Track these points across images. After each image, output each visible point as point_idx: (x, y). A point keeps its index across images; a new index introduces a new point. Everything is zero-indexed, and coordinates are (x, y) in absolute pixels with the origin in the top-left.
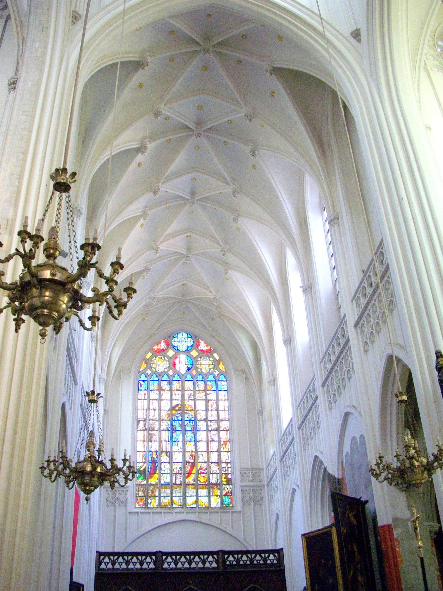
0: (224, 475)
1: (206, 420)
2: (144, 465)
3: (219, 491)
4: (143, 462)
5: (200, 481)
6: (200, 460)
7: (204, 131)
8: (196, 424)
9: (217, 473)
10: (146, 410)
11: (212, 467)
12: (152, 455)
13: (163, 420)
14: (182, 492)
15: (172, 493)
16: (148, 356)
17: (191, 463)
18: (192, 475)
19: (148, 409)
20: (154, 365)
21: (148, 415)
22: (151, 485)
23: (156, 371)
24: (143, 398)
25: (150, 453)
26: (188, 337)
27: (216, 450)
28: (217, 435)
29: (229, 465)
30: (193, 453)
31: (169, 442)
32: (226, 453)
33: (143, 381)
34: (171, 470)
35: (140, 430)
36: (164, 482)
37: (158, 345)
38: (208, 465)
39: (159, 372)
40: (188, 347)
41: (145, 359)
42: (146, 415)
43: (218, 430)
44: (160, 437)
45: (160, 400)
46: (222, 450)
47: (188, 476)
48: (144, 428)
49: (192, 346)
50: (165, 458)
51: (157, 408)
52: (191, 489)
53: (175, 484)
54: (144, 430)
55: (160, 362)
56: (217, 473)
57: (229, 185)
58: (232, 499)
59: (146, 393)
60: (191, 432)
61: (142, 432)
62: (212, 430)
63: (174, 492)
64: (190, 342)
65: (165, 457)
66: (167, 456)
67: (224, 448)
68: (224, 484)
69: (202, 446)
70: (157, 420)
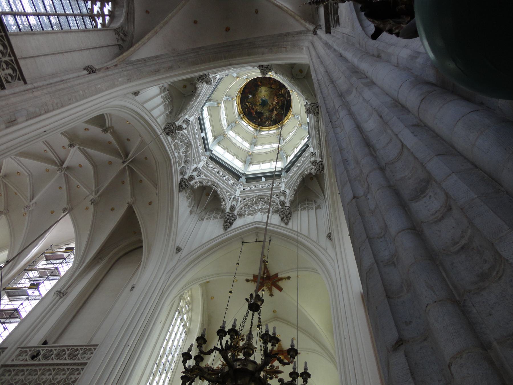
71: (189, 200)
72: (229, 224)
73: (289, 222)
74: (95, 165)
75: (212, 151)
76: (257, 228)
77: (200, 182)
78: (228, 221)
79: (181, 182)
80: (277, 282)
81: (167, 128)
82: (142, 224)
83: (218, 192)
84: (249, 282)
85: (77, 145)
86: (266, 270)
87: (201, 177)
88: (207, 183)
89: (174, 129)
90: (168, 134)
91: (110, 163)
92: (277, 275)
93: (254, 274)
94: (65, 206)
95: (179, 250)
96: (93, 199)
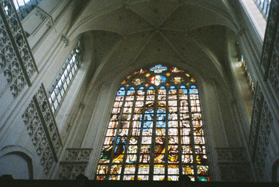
1: (177, 113)
2: (110, 147)
3: (193, 170)
5: (170, 161)
10: (121, 108)
11: (183, 148)
13: (135, 113)
14: (148, 170)
15: (137, 171)
17: (161, 144)
22: (115, 164)
24: (119, 100)
27: (188, 134)
28: (189, 123)
29: (204, 147)
31: (140, 129)
34: (139, 150)
36: (130, 161)
42: (120, 111)
43: (190, 120)
45: (134, 101)
46: (195, 134)
48: (117, 119)
52: (159, 168)
53: (142, 163)
54: (115, 121)
62: (183, 120)
63: (139, 170)
65: (134, 140)
66: (136, 139)
67: (197, 133)
69: (173, 132)
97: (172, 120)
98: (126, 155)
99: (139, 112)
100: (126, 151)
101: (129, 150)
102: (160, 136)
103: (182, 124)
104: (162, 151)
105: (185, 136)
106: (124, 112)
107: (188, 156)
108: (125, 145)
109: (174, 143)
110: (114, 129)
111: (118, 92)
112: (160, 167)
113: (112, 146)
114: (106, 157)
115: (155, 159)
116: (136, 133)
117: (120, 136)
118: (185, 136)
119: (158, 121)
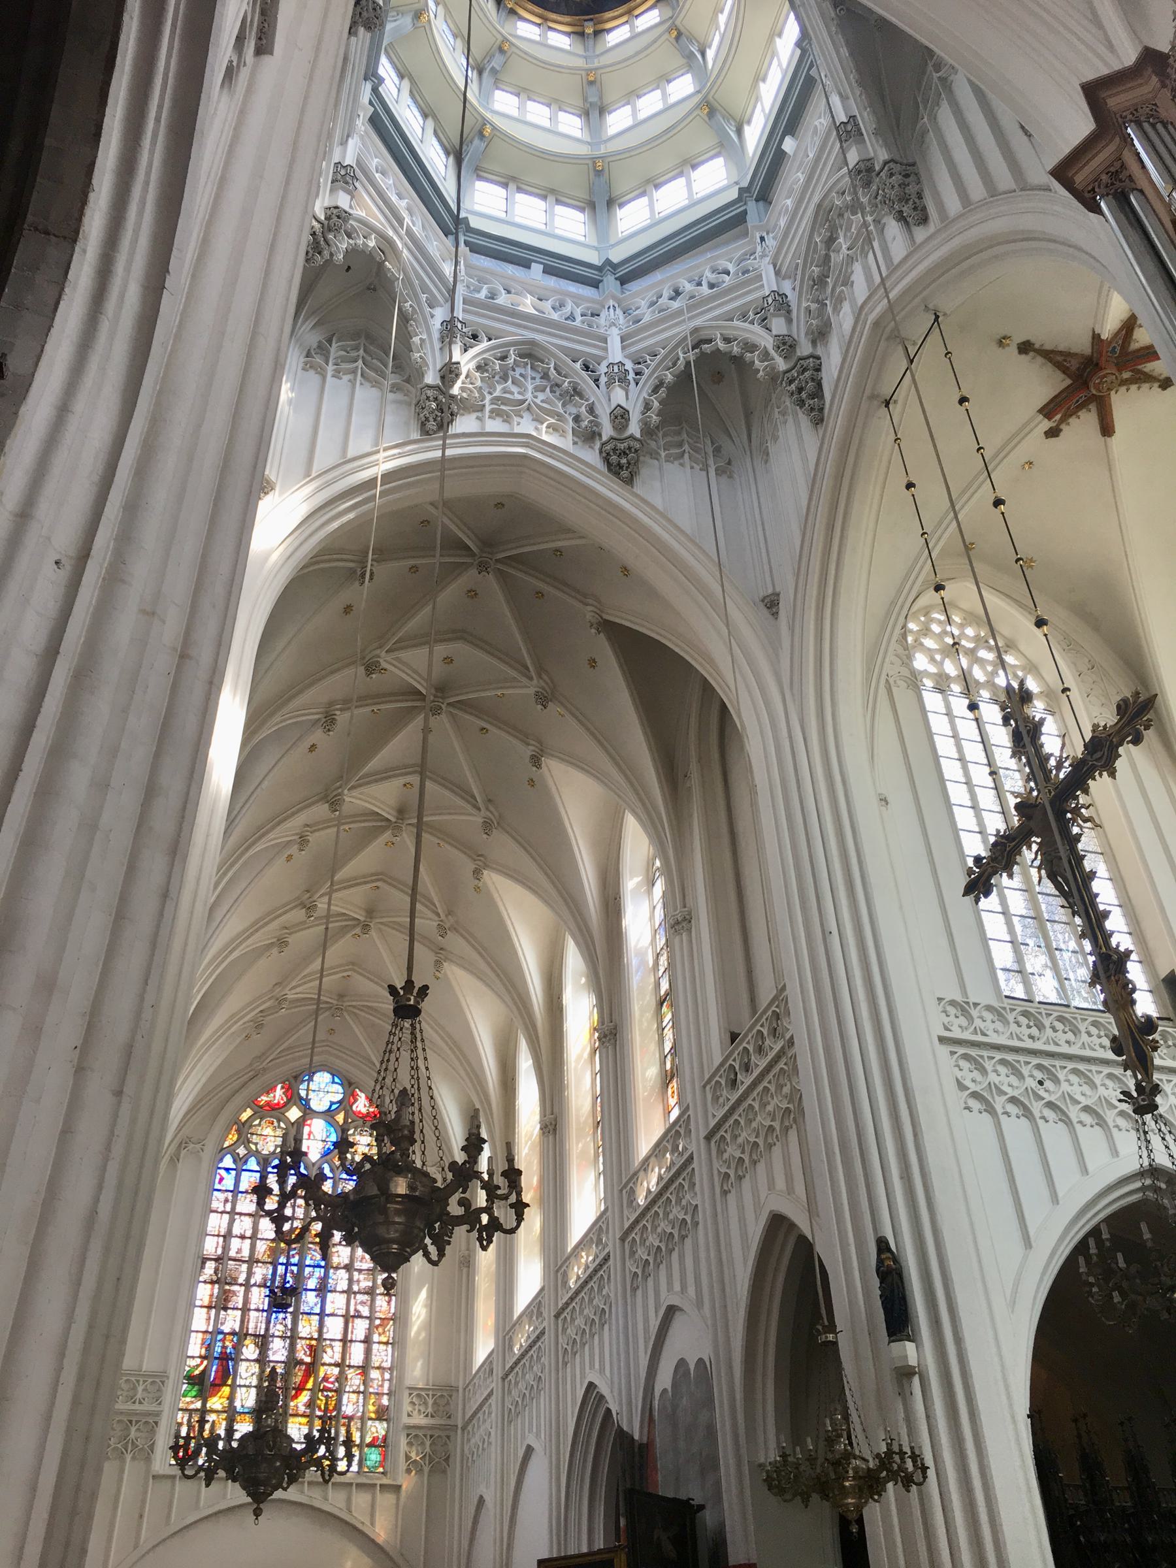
0: (373, 1396)
2: (202, 1363)
4: (200, 1357)
6: (326, 1359)
7: (448, 704)
8: (326, 1275)
9: (359, 1392)
10: (224, 1237)
11: (349, 1377)
12: (223, 1340)
13: (258, 1261)
16: (245, 1116)
17: (306, 1364)
18: (305, 1393)
19: (227, 1236)
20: (254, 1137)
21: (226, 1248)
22: (213, 1411)
23: (257, 1151)
25: (220, 1337)
26: (333, 1082)
27: (362, 1338)
28: (369, 1302)
30: (314, 1343)
32: (383, 1347)
33: (227, 1170)
35: (205, 1282)
36: (242, 1406)
37: (268, 1093)
38: (342, 1372)
39: (264, 1152)
40: (332, 1103)
41: (237, 1121)
42: (224, 1248)
44: (246, 1301)
46: (376, 1338)
47: (296, 1397)
48: (215, 1278)
49: (340, 1102)
50: (250, 1351)
51: (248, 1234)
54: (212, 1282)
55: (268, 1131)
56: (359, 1392)
57: (479, 809)
58: (384, 1456)
59: (230, 1198)
60: (314, 1293)
61: (209, 1286)
62: (359, 1292)
64: (336, 1093)
65: (252, 1347)
66: (256, 1344)
67: (380, 1335)
68: (371, 1419)
69: (334, 1328)
70: (244, 1262)
71: (686, 456)
72: (811, 402)
73: (924, 209)
74: (460, 634)
75: (608, 262)
76: (876, 324)
77: (655, 390)
78: (804, 395)
79: (607, 460)
80: (1129, 343)
81: (427, 419)
82: (658, 633)
83: (722, 346)
84: (1062, 434)
85: (378, 652)
86: (1055, 358)
87: (646, 371)
88: (674, 364)
89: (441, 397)
90: (442, 426)
91: (472, 593)
92: (1096, 337)
93: (1040, 405)
94: (528, 751)
95: (771, 604)
96: (537, 694)
97: (335, 1291)
98: (233, 1387)
99: (266, 1259)
100: (234, 1380)
101: (241, 1378)
102: (306, 1338)
103: (356, 1304)
104: (307, 1382)
105: (356, 1341)
106: (232, 1254)
107: (354, 1397)
108: (232, 1359)
109: (332, 1361)
110: (209, 1307)
111: (218, 1177)
112: (300, 1424)
113: (205, 1362)
114: (194, 1393)
115: (292, 1404)
116: (256, 1328)
117: (222, 1332)
118: (356, 1341)
119: (306, 1290)
